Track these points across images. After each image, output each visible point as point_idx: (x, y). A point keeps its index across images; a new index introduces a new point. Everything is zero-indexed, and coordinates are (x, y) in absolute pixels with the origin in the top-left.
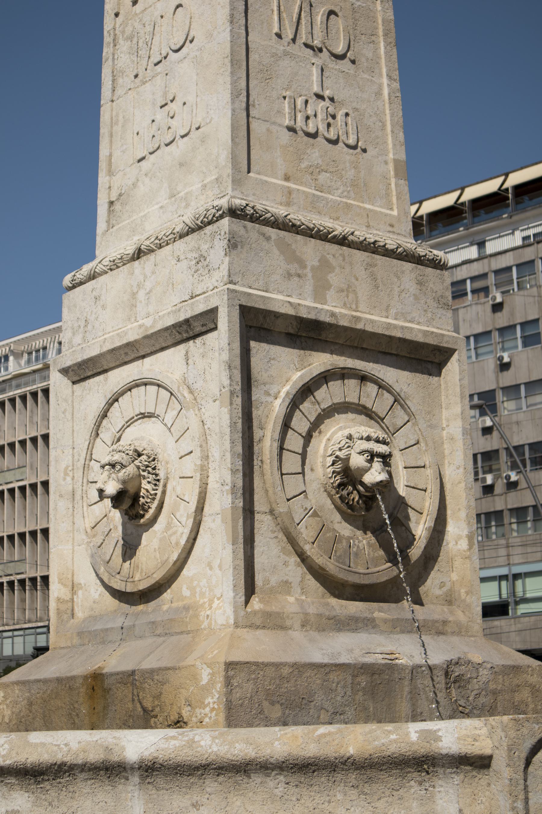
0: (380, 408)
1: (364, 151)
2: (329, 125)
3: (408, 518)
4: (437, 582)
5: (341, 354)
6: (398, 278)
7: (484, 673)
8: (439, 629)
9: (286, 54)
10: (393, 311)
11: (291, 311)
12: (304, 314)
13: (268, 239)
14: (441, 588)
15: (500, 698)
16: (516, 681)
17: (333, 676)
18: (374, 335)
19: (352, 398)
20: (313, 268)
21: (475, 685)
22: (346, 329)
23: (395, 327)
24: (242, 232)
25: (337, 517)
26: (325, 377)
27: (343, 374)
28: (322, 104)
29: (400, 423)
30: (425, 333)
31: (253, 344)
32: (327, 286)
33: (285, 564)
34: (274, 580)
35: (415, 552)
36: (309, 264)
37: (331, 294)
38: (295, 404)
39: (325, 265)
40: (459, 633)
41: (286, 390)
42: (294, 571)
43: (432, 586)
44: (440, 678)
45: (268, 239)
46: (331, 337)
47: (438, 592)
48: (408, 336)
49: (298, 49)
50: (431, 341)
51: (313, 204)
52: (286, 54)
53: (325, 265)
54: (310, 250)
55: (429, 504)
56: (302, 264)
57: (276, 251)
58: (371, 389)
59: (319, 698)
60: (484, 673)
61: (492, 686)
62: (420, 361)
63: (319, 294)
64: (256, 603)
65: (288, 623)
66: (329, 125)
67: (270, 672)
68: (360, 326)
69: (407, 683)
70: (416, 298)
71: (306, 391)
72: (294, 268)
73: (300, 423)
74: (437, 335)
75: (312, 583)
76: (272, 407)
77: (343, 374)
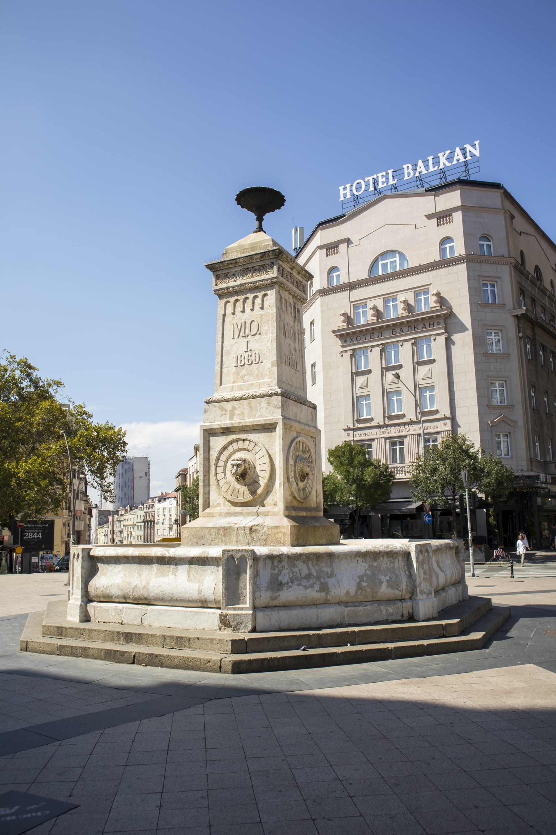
0: (250, 448)
1: (262, 362)
2: (249, 360)
3: (259, 480)
4: (271, 499)
5: (239, 434)
6: (260, 404)
7: (265, 529)
8: (266, 514)
9: (236, 343)
10: (257, 416)
11: (219, 427)
12: (223, 426)
13: (215, 407)
14: (272, 500)
15: (270, 536)
16: (277, 531)
17: (212, 531)
18: (246, 426)
19: (241, 447)
20: (230, 411)
21: (261, 532)
22: (237, 427)
23: (254, 421)
24: (208, 407)
25: (236, 483)
26: (231, 443)
27: (237, 441)
28: (247, 353)
29: (257, 451)
30: (265, 420)
31: (211, 438)
32: (234, 414)
33: (219, 498)
34: (215, 503)
35: (259, 491)
36: (228, 410)
37: (235, 417)
38: (221, 453)
39: (234, 408)
40: (274, 515)
41: (218, 449)
42: (222, 501)
43: (269, 500)
44: (248, 531)
45: (215, 407)
46: (234, 430)
47: (271, 502)
48: (259, 423)
49: (241, 339)
50: (268, 422)
51: (240, 388)
52: (236, 343)
53: (234, 408)
54: (228, 406)
55: (267, 475)
56: (226, 411)
57: (218, 409)
58: (247, 443)
59: (208, 536)
60: (265, 529)
61: (267, 533)
62: (268, 429)
63: (231, 418)
64: (207, 510)
65: (215, 515)
66: (249, 360)
67: (194, 530)
68: (241, 425)
69: (235, 532)
70: (266, 408)
71: (225, 448)
72: (223, 413)
73: (223, 458)
74: (270, 419)
75: (227, 503)
76: (214, 454)
77: (237, 441)
